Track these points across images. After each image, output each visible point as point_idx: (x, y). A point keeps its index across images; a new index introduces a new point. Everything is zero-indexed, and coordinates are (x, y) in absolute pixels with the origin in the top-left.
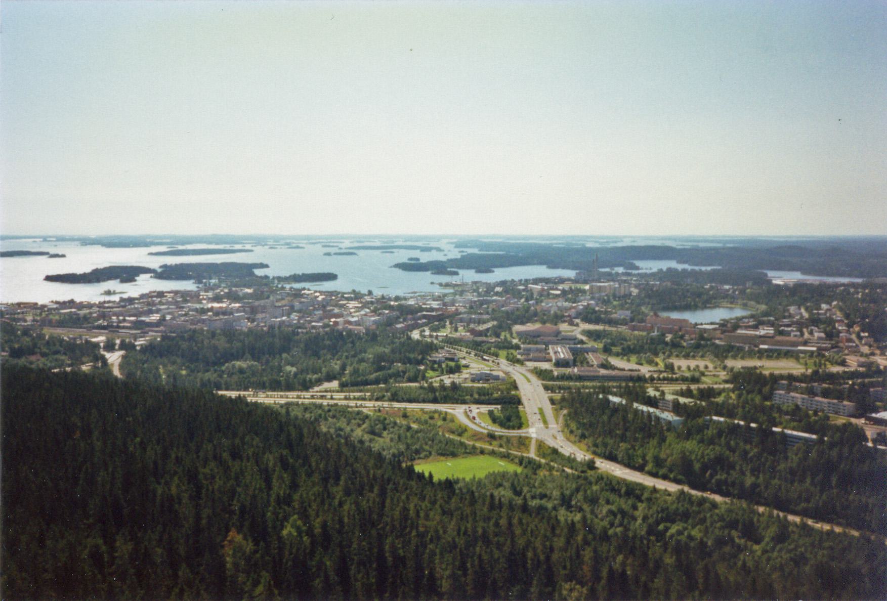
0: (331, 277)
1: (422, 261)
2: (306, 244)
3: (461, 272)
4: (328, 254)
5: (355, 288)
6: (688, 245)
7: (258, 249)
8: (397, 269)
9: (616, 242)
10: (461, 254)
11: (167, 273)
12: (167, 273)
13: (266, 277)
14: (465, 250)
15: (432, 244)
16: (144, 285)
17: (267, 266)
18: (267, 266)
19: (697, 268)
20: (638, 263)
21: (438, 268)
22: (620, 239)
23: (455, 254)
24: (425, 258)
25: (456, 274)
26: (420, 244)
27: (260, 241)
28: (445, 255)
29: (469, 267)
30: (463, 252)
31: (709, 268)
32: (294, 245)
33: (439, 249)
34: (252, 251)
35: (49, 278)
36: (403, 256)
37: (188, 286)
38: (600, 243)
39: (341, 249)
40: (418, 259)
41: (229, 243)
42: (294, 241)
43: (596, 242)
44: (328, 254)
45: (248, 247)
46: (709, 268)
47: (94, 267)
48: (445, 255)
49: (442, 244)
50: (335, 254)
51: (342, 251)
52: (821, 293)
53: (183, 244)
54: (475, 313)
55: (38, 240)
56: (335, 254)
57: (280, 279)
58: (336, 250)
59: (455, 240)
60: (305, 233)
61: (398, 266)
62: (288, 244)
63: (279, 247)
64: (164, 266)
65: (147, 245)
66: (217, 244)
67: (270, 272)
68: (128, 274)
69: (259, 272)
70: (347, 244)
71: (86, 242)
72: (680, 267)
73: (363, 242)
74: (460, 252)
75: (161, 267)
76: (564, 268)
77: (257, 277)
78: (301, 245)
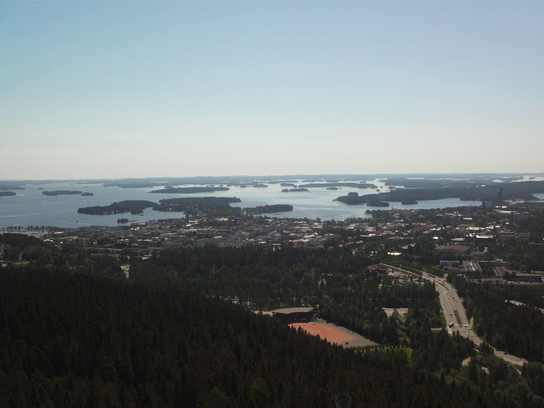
2: (269, 183)
11: (163, 206)
13: (238, 209)
15: (368, 182)
17: (238, 200)
20: (535, 195)
21: (372, 200)
23: (385, 189)
24: (361, 193)
26: (358, 182)
29: (396, 200)
30: (393, 188)
33: (373, 187)
35: (82, 211)
36: (344, 192)
37: (180, 215)
39: (296, 186)
42: (260, 181)
44: (286, 191)
45: (225, 186)
47: (113, 202)
49: (376, 182)
50: (291, 190)
53: (176, 185)
54: (403, 236)
55: (74, 183)
56: (291, 190)
58: (292, 188)
59: (386, 179)
61: (340, 199)
63: (248, 186)
64: (163, 201)
65: (151, 186)
66: (201, 184)
67: (242, 206)
69: (233, 205)
70: (300, 183)
73: (313, 181)
76: (473, 200)
78: (264, 184)
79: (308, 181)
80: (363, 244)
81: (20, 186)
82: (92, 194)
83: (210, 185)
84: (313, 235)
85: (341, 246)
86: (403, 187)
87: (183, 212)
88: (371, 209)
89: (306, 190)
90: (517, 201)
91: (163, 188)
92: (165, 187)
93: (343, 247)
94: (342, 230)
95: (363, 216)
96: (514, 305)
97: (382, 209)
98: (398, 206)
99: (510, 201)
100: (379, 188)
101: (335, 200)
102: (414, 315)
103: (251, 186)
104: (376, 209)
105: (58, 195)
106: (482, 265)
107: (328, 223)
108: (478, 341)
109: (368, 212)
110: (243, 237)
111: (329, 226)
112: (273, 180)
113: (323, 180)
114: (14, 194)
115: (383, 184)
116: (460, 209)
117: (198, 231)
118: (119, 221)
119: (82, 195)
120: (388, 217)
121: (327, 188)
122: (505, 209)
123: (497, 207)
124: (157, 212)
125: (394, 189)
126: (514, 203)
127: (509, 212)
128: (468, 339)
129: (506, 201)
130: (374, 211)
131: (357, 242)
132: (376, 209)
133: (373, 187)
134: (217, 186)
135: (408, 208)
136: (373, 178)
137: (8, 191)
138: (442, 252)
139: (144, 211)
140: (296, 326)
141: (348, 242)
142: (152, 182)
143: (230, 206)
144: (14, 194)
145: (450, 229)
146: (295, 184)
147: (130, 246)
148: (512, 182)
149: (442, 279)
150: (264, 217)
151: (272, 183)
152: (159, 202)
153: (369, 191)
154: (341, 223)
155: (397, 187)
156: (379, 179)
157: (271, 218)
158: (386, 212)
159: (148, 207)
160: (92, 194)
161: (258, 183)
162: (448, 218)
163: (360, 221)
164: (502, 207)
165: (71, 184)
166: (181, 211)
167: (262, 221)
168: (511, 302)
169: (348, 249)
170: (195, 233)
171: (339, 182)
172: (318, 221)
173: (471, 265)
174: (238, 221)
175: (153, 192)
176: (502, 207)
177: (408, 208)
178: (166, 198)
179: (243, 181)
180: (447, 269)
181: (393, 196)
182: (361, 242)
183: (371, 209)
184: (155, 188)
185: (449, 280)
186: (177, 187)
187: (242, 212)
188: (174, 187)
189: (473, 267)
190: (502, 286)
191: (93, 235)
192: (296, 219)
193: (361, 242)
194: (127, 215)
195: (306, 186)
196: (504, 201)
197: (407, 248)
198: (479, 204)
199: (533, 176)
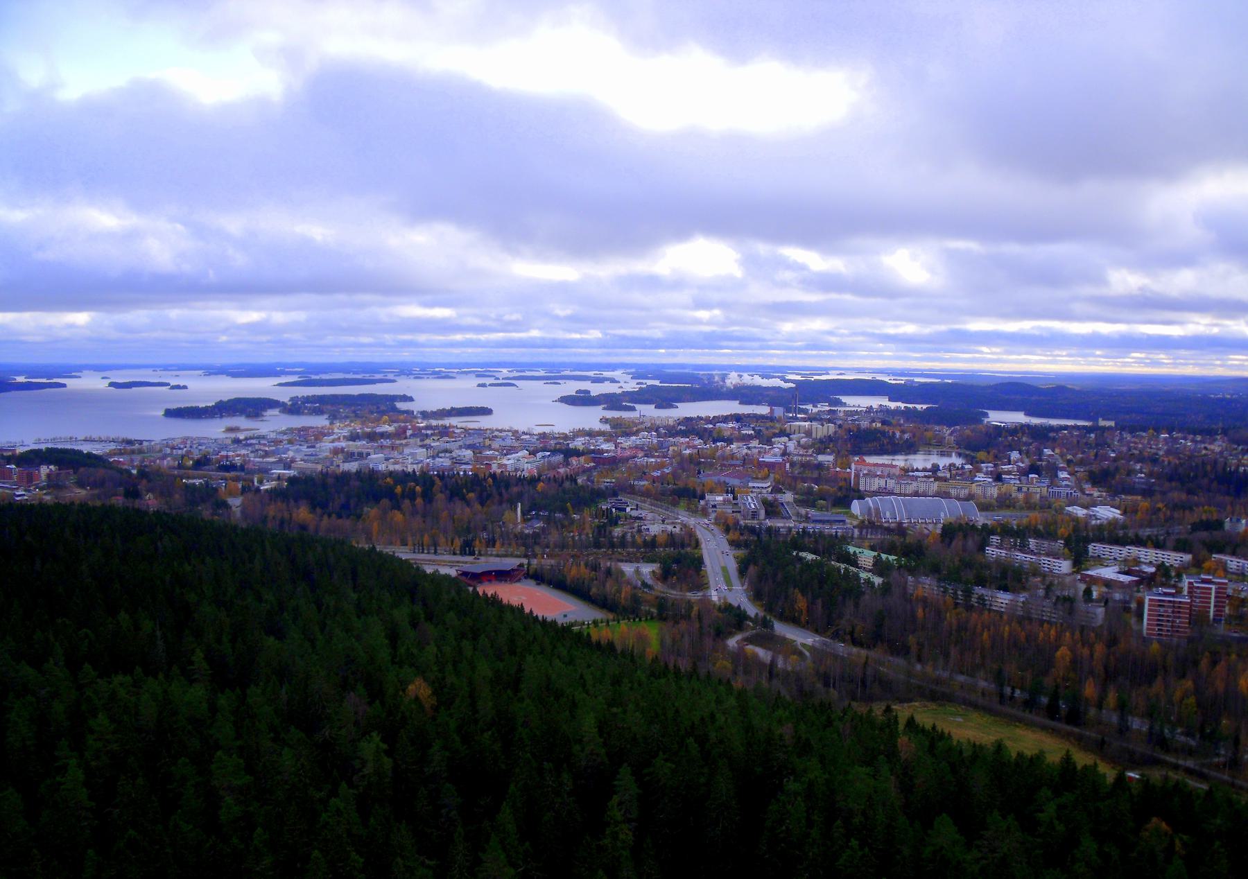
0: (486, 411)
1: (593, 394)
3: (638, 407)
4: (483, 385)
5: (512, 426)
6: (902, 381)
10: (639, 386)
11: (294, 408)
14: (644, 381)
15: (606, 374)
17: (411, 399)
19: (910, 406)
20: (844, 399)
21: (611, 401)
23: (631, 386)
24: (596, 390)
25: (633, 409)
26: (591, 374)
27: (406, 371)
30: (642, 383)
32: (443, 374)
33: (613, 381)
34: (393, 381)
35: (170, 413)
36: (571, 388)
39: (498, 379)
40: (588, 392)
41: (370, 373)
44: (483, 385)
45: (390, 376)
50: (490, 385)
52: (1041, 435)
53: (317, 374)
55: (158, 370)
56: (490, 385)
57: (425, 415)
58: (492, 381)
59: (633, 370)
62: (434, 373)
63: (426, 376)
64: (294, 400)
66: (355, 373)
67: (415, 407)
68: (254, 407)
69: (401, 406)
72: (893, 405)
73: (524, 371)
74: (637, 384)
75: (292, 399)
78: (451, 375)
80: (595, 468)
81: (73, 374)
83: (368, 375)
86: (657, 383)
88: (611, 414)
89: (513, 385)
92: (299, 377)
95: (598, 426)
97: (625, 415)
98: (648, 411)
99: (809, 407)
100: (622, 384)
101: (556, 401)
103: (431, 377)
105: (134, 388)
108: (752, 610)
109: (604, 421)
113: (540, 370)
116: (738, 418)
119: (171, 389)
121: (545, 382)
122: (804, 420)
123: (791, 415)
125: (645, 386)
126: (815, 410)
128: (739, 607)
129: (804, 407)
131: (586, 465)
133: (613, 381)
136: (613, 367)
137: (55, 380)
139: (265, 414)
142: (278, 369)
143: (397, 408)
146: (497, 375)
148: (813, 379)
150: (448, 425)
152: (290, 401)
155: (650, 382)
157: (458, 426)
163: (591, 434)
164: (798, 416)
165: (154, 371)
167: (445, 432)
168: (800, 554)
169: (573, 480)
171: (563, 373)
174: (407, 431)
175: (280, 385)
176: (798, 416)
179: (418, 369)
183: (611, 414)
188: (314, 377)
191: (186, 451)
194: (241, 422)
195: (514, 378)
196: (801, 407)
197: (659, 474)
199: (843, 372)
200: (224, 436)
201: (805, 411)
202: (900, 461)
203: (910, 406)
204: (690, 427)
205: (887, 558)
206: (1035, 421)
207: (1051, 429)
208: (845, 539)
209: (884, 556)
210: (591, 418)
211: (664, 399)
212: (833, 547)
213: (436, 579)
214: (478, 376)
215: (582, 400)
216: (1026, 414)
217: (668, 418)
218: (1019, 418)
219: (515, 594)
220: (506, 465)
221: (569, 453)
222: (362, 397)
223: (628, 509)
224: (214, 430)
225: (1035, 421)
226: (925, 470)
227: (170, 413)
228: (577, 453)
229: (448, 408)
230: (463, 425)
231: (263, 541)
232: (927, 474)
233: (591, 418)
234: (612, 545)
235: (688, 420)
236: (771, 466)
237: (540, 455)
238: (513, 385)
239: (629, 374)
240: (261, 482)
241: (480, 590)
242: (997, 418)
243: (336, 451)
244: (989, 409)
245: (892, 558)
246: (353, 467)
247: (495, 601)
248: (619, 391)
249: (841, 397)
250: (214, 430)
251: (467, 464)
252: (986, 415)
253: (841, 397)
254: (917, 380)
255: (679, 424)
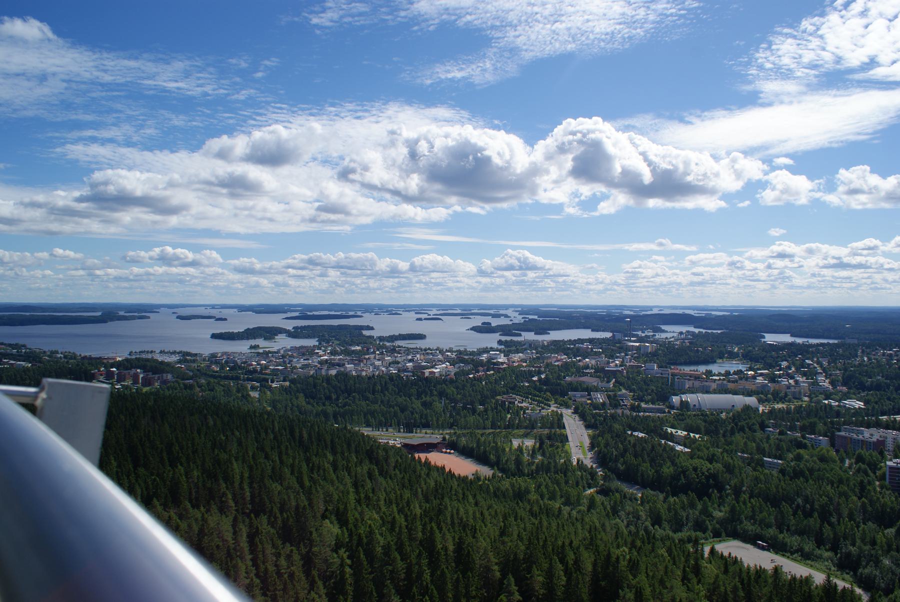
0: (421, 337)
1: (493, 325)
3: (523, 333)
6: (703, 314)
7: (366, 315)
8: (473, 332)
9: (646, 311)
11: (295, 334)
12: (295, 334)
13: (371, 337)
14: (527, 316)
15: (502, 312)
16: (282, 343)
17: (372, 328)
18: (372, 328)
19: (710, 331)
20: (664, 327)
21: (505, 330)
22: (651, 308)
23: (519, 319)
24: (495, 322)
25: (520, 335)
26: (491, 312)
27: (368, 309)
28: (511, 320)
31: (719, 332)
33: (506, 316)
35: (214, 336)
36: (478, 321)
38: (635, 311)
40: (490, 324)
41: (345, 311)
43: (631, 311)
45: (359, 313)
46: (719, 332)
48: (511, 320)
49: (509, 312)
50: (426, 319)
51: (432, 317)
52: (804, 350)
54: (533, 367)
56: (426, 319)
57: (381, 339)
58: (426, 316)
59: (520, 309)
60: (402, 303)
61: (475, 329)
65: (285, 312)
67: (375, 334)
68: (270, 333)
69: (366, 333)
70: (434, 311)
71: (242, 308)
72: (697, 331)
73: (447, 310)
75: (294, 328)
76: (603, 331)
77: (364, 336)
79: (443, 310)
82: (225, 319)
84: (444, 365)
85: (471, 376)
86: (536, 317)
87: (317, 339)
88: (504, 338)
89: (440, 319)
90: (646, 333)
91: (297, 314)
93: (474, 377)
94: (473, 360)
95: (495, 345)
96: (637, 436)
98: (529, 336)
102: (541, 447)
104: (508, 338)
106: (609, 397)
107: (459, 352)
109: (500, 342)
110: (376, 367)
111: (460, 356)
112: (408, 308)
114: (149, 317)
115: (516, 314)
116: (591, 341)
117: (331, 359)
118: (252, 347)
120: (518, 347)
122: (634, 341)
124: (290, 339)
126: (643, 335)
127: (638, 344)
130: (506, 341)
132: (508, 338)
134: (351, 313)
135: (540, 338)
136: (507, 307)
138: (570, 384)
139: (276, 337)
140: (423, 456)
141: (478, 372)
144: (149, 317)
145: (580, 361)
146: (429, 312)
147: (261, 373)
149: (570, 411)
151: (406, 311)
153: (505, 322)
154: (472, 353)
155: (531, 317)
156: (513, 309)
158: (519, 343)
159: (281, 333)
160: (225, 319)
161: (391, 311)
162: (578, 349)
166: (314, 337)
167: (393, 351)
170: (327, 360)
171: (473, 311)
172: (450, 350)
173: (599, 396)
177: (540, 338)
178: (299, 325)
180: (575, 401)
181: (527, 326)
182: (492, 372)
183: (504, 338)
184: (289, 315)
185: (576, 412)
186: (311, 314)
187: (375, 340)
188: (309, 313)
189: (600, 398)
190: (627, 417)
192: (429, 349)
193: (492, 372)
194: (261, 342)
198: (608, 335)
200: (249, 351)
201: (636, 336)
202: (702, 369)
203: (710, 331)
204: (558, 346)
205: (694, 436)
206: (799, 341)
207: (811, 346)
208: (662, 422)
209: (692, 435)
210: (491, 341)
211: (541, 330)
212: (655, 429)
213: (387, 448)
214: (416, 313)
215: (486, 329)
216: (791, 336)
217: (543, 341)
218: (786, 338)
219: (436, 458)
220: (435, 372)
221: (477, 365)
222: (340, 327)
223: (516, 402)
224: (242, 348)
225: (799, 341)
226: (719, 374)
227: (214, 336)
228: (481, 364)
229: (397, 334)
230: (407, 346)
231: (273, 422)
232: (722, 378)
233: (491, 341)
234: (507, 427)
235: (555, 343)
236: (614, 373)
237: (457, 365)
238: (440, 319)
239: (516, 311)
240: (272, 382)
241: (416, 455)
242: (770, 338)
243: (321, 363)
244: (767, 333)
245: (697, 436)
246: (333, 372)
247: (427, 463)
248: (510, 323)
249: (661, 326)
250: (242, 348)
251: (409, 371)
252: (764, 337)
253: (661, 326)
254: (713, 313)
255: (551, 345)
